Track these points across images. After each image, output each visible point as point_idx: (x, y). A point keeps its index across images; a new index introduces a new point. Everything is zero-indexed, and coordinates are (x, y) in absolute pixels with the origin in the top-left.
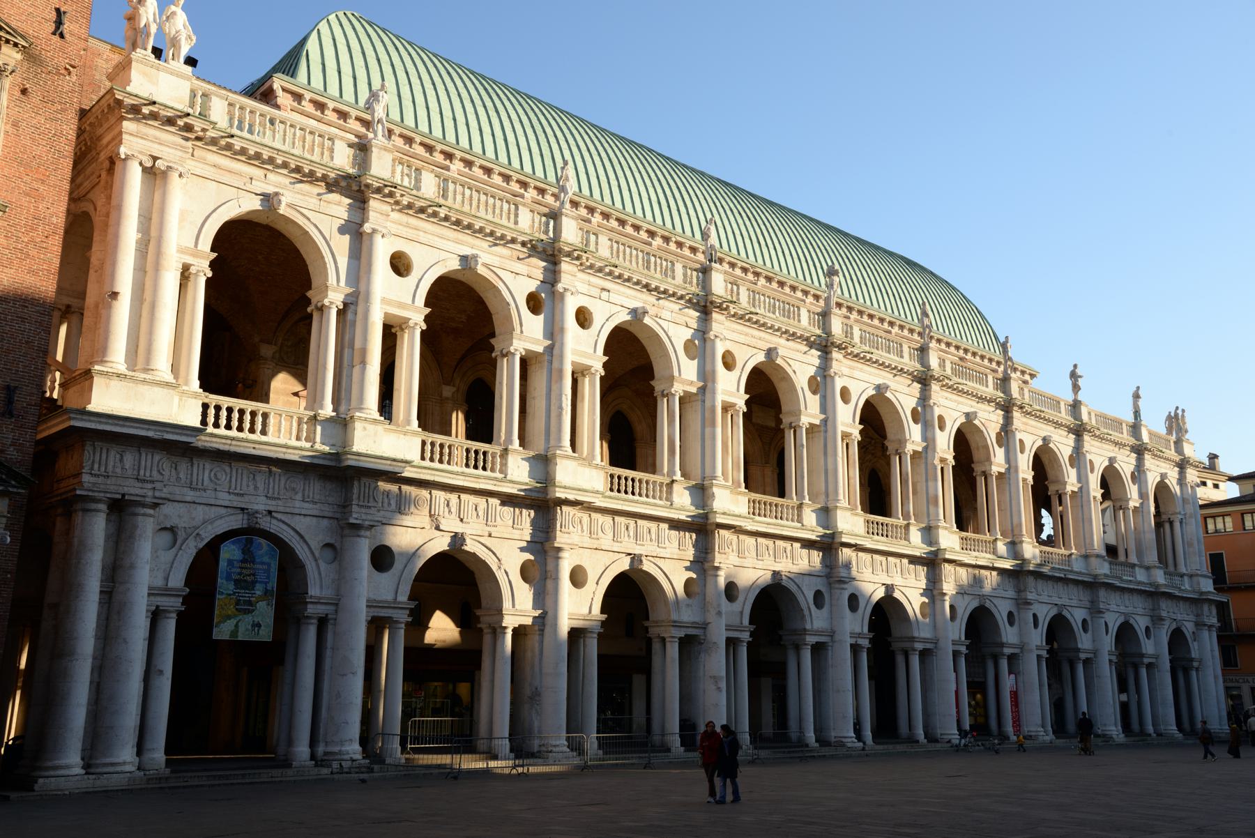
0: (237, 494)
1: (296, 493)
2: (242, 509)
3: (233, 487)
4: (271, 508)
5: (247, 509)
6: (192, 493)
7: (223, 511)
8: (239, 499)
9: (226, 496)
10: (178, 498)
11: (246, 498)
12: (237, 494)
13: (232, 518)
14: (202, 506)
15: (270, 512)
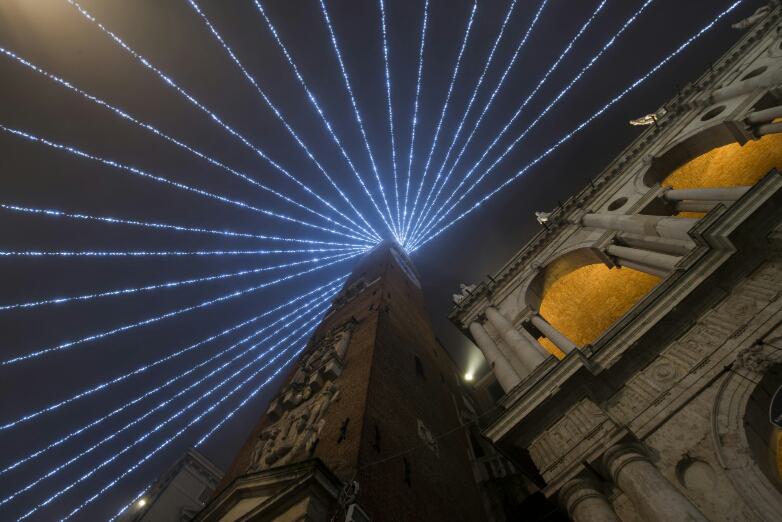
0: (700, 366)
1: (755, 305)
2: (727, 369)
3: (686, 365)
4: (757, 337)
5: (731, 365)
6: (659, 407)
7: (714, 391)
8: (707, 367)
9: (693, 378)
10: (654, 424)
11: (715, 359)
12: (700, 366)
13: (732, 385)
14: (686, 408)
15: (760, 342)
